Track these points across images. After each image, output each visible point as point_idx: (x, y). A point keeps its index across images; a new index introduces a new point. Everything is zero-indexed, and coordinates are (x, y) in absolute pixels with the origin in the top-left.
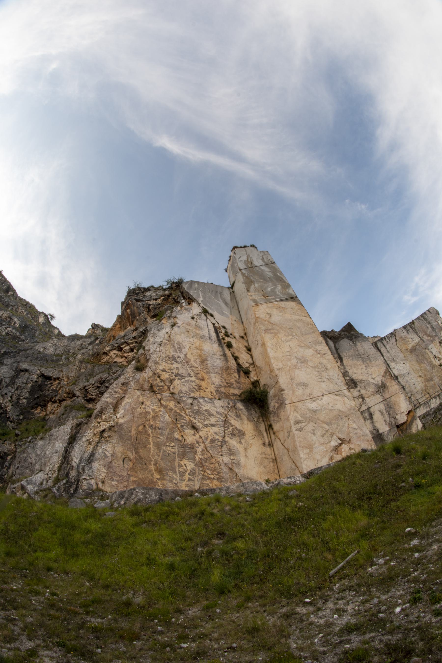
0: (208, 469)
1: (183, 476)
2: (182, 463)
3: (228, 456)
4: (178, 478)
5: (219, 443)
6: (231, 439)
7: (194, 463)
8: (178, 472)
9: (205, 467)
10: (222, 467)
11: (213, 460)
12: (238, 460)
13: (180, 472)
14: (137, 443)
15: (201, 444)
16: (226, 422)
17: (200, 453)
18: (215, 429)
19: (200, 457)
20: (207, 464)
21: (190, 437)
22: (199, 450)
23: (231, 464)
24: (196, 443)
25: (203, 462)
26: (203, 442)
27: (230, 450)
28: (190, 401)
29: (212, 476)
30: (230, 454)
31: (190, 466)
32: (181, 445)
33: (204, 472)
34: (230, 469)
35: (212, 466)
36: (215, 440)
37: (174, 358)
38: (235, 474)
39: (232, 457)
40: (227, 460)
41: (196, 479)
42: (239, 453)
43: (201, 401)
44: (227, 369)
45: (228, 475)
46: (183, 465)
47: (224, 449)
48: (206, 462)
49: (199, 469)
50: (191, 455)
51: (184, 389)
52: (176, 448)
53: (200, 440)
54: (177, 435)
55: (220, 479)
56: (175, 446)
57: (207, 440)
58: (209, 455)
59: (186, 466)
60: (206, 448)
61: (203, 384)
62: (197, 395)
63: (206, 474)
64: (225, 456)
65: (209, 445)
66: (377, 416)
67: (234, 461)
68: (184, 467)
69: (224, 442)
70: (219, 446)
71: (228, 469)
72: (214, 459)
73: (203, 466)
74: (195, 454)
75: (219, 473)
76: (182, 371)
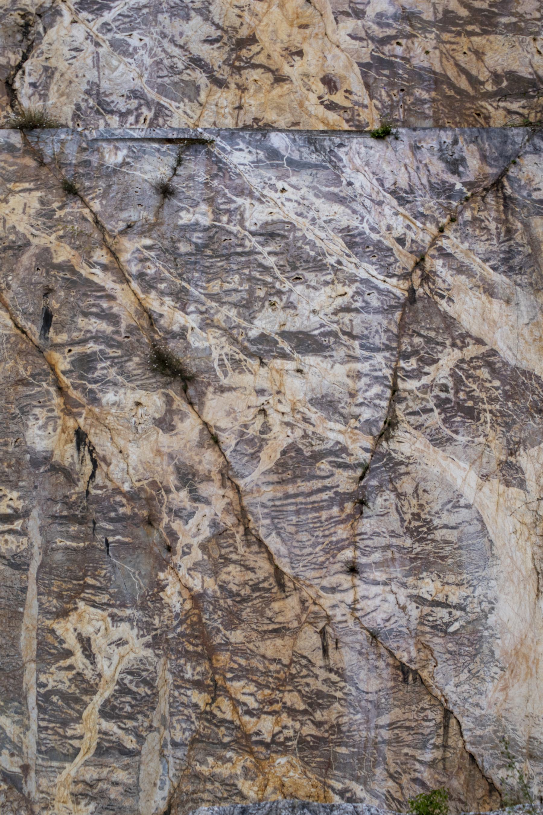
0: (244, 673)
1: (65, 724)
2: (66, 630)
3: (397, 572)
4: (30, 741)
5: (345, 481)
6: (438, 441)
7: (148, 627)
8: (32, 700)
9: (223, 659)
10: (346, 658)
11: (288, 609)
12: (474, 608)
13: (45, 697)
15: (205, 490)
16: (417, 312)
17: (197, 555)
18: (326, 373)
19: (196, 583)
20: (237, 636)
21: (135, 438)
22: (193, 532)
23: (417, 635)
24: (172, 480)
25: (214, 620)
26: (227, 476)
27: (420, 528)
28: (155, 168)
29: (266, 726)
30: (420, 564)
31: (116, 652)
32: (66, 501)
33: (216, 691)
34: (404, 672)
35: (271, 647)
36: (317, 457)
38: (438, 717)
39: (429, 587)
40: (389, 607)
41: (153, 740)
42: (489, 555)
43: (240, 157)
45: (384, 720)
46: (72, 642)
47: (381, 521)
48: (233, 620)
49: (178, 673)
50: (130, 574)
51: (123, 76)
52: (34, 523)
53: (208, 461)
54: (42, 436)
55: (320, 751)
56: (26, 514)
57: (255, 457)
58: (264, 568)
59: (90, 655)
60: (243, 516)
62: (215, 110)
63: (225, 710)
64: (379, 576)
65: (268, 493)
67: (442, 613)
68: (79, 660)
69: (383, 467)
70: (340, 499)
71: (387, 673)
72: (293, 602)
73: (209, 653)
74: (163, 564)
75: (316, 701)
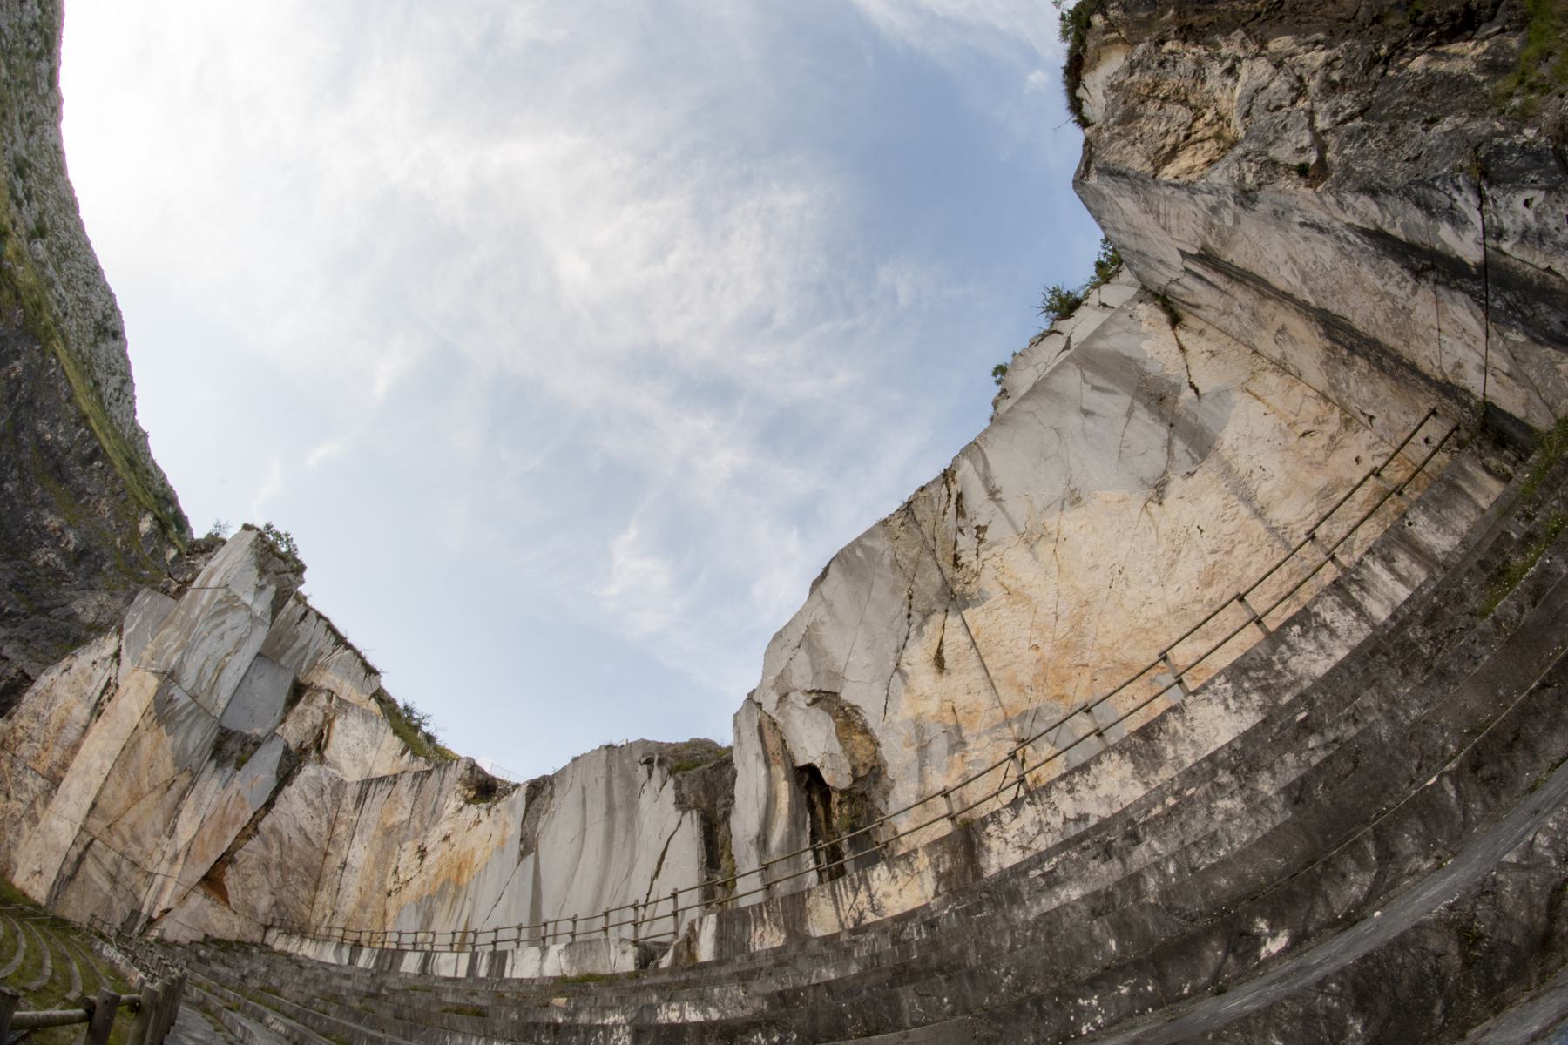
16: (33, 803)
18: (20, 805)
37: (37, 715)
51: (26, 754)
61: (44, 755)
62: (31, 764)
69: (19, 821)
76: (35, 734)
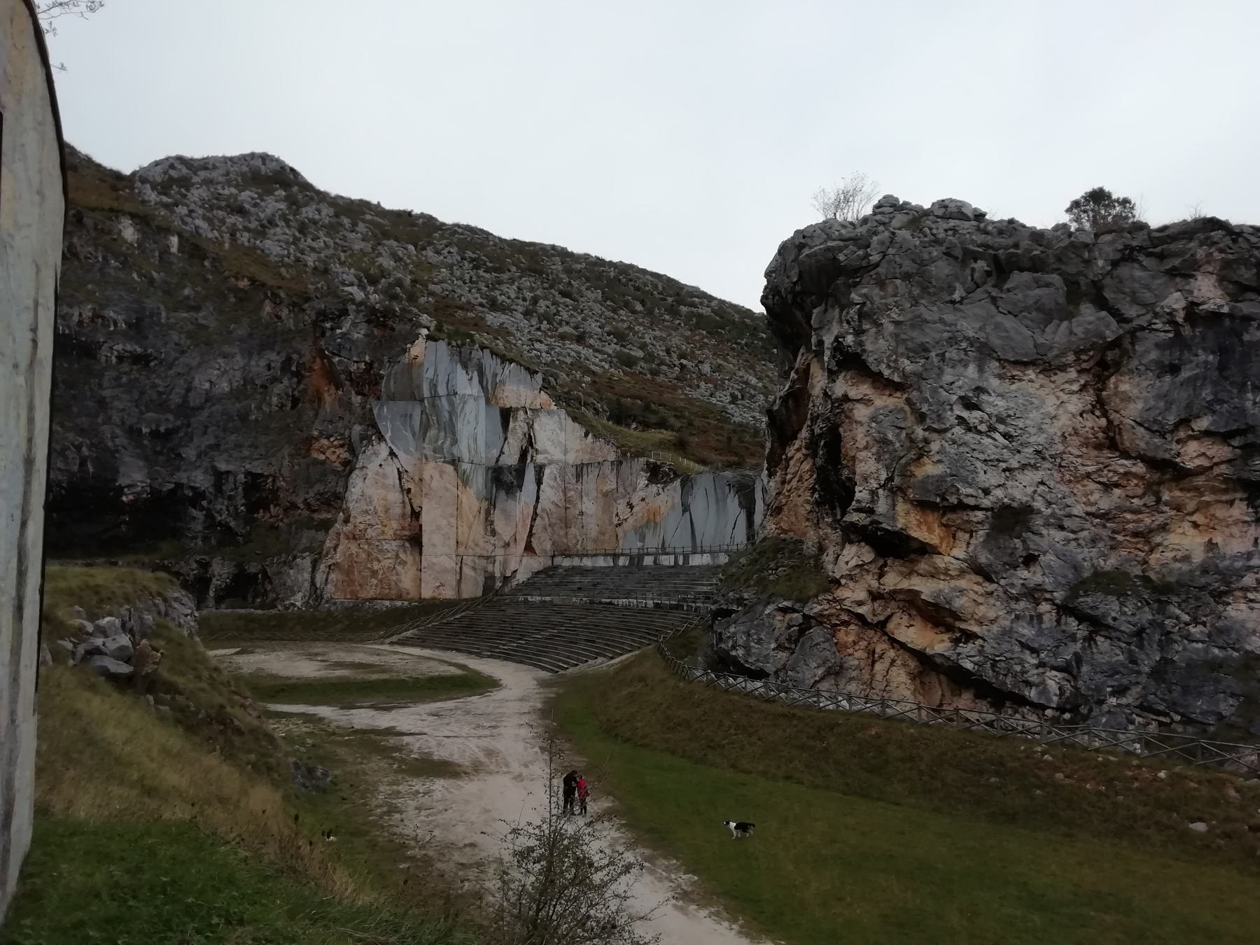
14: (348, 572)
16: (397, 556)
21: (376, 566)
37: (367, 512)
44: (404, 515)
61: (386, 529)
66: (497, 563)
76: (372, 522)
